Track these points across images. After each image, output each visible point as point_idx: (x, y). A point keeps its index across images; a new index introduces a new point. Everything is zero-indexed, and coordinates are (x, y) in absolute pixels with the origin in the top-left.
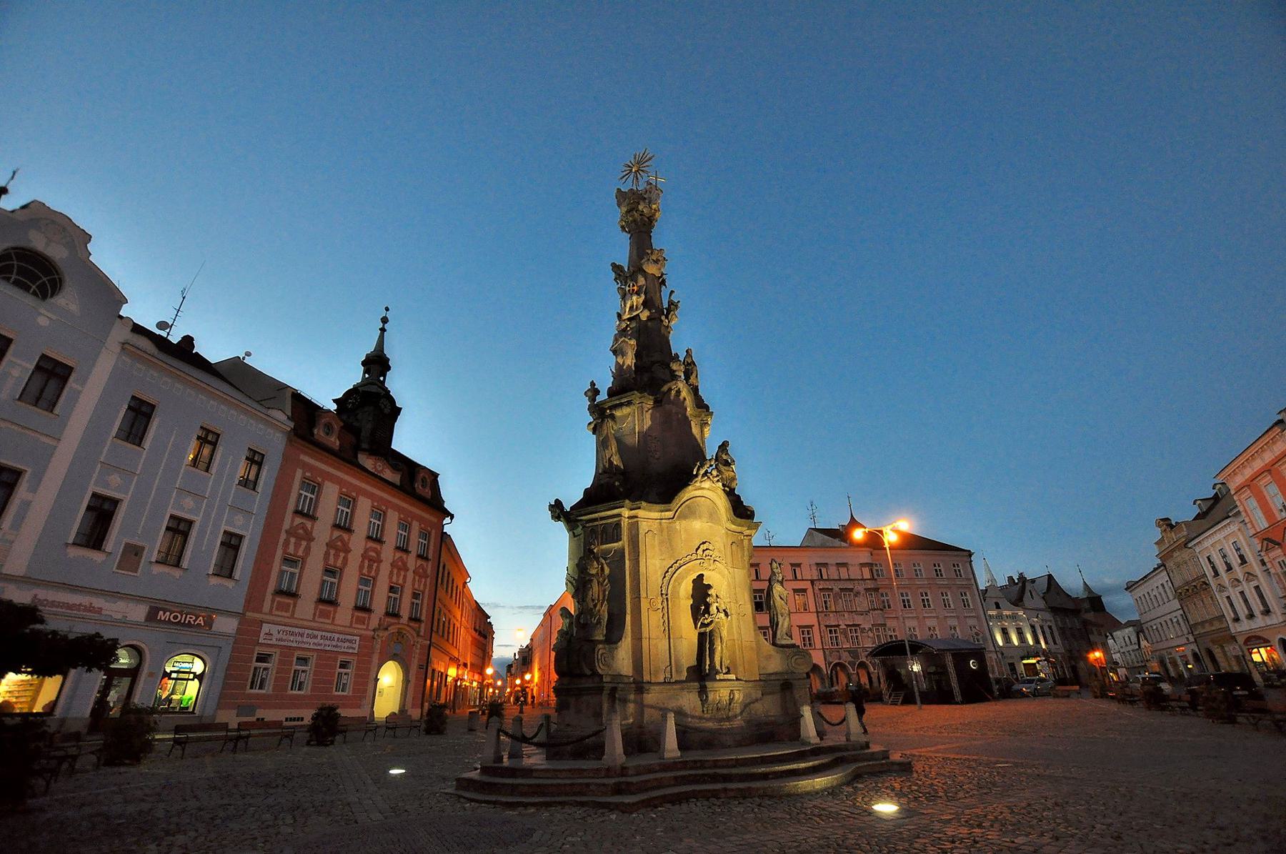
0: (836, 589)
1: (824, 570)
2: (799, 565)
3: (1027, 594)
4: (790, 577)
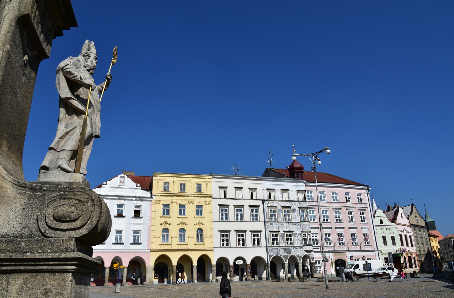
0: (279, 207)
1: (272, 194)
2: (256, 189)
3: (399, 215)
4: (249, 197)
